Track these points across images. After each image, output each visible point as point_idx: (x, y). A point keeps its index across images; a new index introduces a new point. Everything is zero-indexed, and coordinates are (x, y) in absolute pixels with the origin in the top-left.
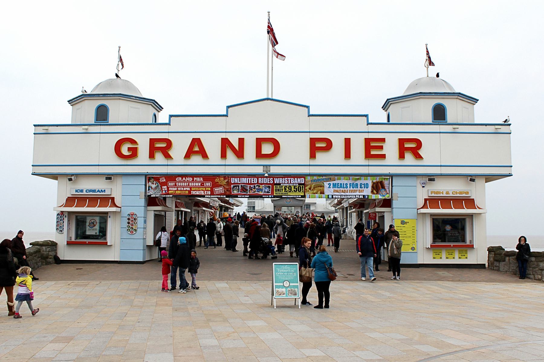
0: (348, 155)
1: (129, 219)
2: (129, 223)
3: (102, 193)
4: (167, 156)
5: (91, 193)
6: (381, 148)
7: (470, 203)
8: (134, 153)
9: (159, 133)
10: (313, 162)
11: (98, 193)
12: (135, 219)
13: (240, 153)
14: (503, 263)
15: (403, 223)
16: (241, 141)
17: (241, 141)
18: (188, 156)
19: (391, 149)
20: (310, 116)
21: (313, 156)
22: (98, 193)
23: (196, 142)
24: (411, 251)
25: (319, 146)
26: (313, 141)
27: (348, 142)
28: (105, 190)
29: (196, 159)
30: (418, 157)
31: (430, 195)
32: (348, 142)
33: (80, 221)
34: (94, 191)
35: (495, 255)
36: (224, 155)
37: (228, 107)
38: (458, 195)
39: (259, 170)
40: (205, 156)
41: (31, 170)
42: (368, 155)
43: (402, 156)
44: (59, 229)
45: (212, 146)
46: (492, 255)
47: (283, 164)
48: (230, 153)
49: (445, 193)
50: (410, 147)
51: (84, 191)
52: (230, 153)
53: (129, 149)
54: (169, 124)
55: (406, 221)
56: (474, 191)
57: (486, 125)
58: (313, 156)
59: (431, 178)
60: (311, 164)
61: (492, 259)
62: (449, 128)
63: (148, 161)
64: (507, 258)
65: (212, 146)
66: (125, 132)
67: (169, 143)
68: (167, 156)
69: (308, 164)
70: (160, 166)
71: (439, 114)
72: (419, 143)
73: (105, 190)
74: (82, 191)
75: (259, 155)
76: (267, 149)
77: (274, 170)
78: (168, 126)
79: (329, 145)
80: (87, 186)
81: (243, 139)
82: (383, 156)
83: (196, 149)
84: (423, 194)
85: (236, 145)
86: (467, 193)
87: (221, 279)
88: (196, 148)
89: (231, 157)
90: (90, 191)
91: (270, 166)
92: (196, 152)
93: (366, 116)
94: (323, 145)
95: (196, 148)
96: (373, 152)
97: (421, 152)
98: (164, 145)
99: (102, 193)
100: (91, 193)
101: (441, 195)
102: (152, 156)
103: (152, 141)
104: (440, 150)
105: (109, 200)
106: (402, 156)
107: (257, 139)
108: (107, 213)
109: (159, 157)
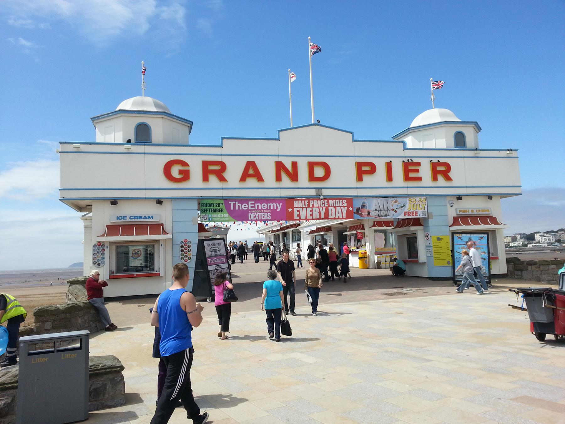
0: (390, 178)
1: (182, 247)
2: (182, 251)
3: (149, 220)
4: (222, 179)
5: (136, 220)
6: (417, 171)
7: (494, 220)
8: (186, 176)
9: (212, 154)
10: (360, 184)
11: (145, 220)
12: (189, 247)
13: (294, 177)
14: (526, 272)
15: (439, 239)
16: (295, 164)
17: (295, 164)
18: (243, 179)
19: (425, 171)
20: (354, 141)
21: (360, 179)
22: (145, 220)
23: (251, 165)
24: (448, 265)
25: (364, 169)
26: (359, 165)
27: (389, 166)
28: (152, 217)
29: (252, 182)
30: (448, 179)
31: (458, 213)
32: (389, 166)
33: (122, 253)
34: (140, 217)
35: (514, 265)
36: (279, 179)
37: (280, 131)
38: (481, 213)
39: (313, 193)
40: (260, 179)
41: (59, 195)
42: (407, 178)
43: (435, 178)
44: (97, 263)
45: (267, 169)
46: (512, 265)
47: (330, 188)
48: (284, 176)
49: (470, 211)
50: (441, 170)
51: (128, 218)
52: (284, 176)
53: (180, 172)
54: (221, 147)
55: (441, 237)
56: (495, 208)
57: (499, 150)
58: (360, 179)
59: (459, 198)
60: (358, 186)
61: (511, 269)
62: (471, 153)
63: (202, 185)
64: (530, 268)
65: (267, 169)
66: (175, 153)
67: (223, 166)
68: (222, 179)
70: (214, 189)
71: (460, 141)
72: (448, 167)
73: (152, 217)
74: (125, 218)
75: (312, 178)
76: (319, 172)
77: (326, 193)
78: (220, 148)
79: (373, 169)
80: (129, 212)
81: (296, 162)
82: (420, 179)
83: (251, 172)
84: (452, 213)
85: (290, 167)
86: (488, 211)
87: (408, 287)
88: (251, 171)
89: (286, 181)
90: (135, 217)
91: (321, 188)
92: (251, 176)
93: (354, 141)
95: (251, 171)
96: (412, 175)
97: (451, 174)
98: (217, 168)
99: (149, 220)
101: (468, 213)
102: (205, 179)
103: (205, 164)
104: (468, 173)
105: (157, 227)
106: (435, 178)
107: (203, 161)
108: (157, 241)
109: (213, 181)
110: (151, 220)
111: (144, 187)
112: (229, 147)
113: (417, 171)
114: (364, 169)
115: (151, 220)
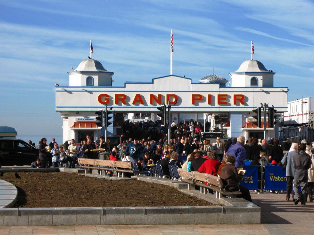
0: (209, 103)
3: (92, 120)
5: (86, 120)
9: (121, 91)
11: (90, 120)
22: (90, 120)
25: (197, 99)
26: (193, 96)
36: (151, 103)
42: (219, 103)
48: (154, 101)
51: (83, 119)
53: (106, 99)
69: (191, 106)
71: (254, 82)
92: (138, 101)
94: (199, 98)
99: (92, 120)
100: (86, 120)
110: (93, 120)
111: (89, 106)
112: (129, 87)
113: (225, 99)
114: (197, 99)
115: (93, 120)
